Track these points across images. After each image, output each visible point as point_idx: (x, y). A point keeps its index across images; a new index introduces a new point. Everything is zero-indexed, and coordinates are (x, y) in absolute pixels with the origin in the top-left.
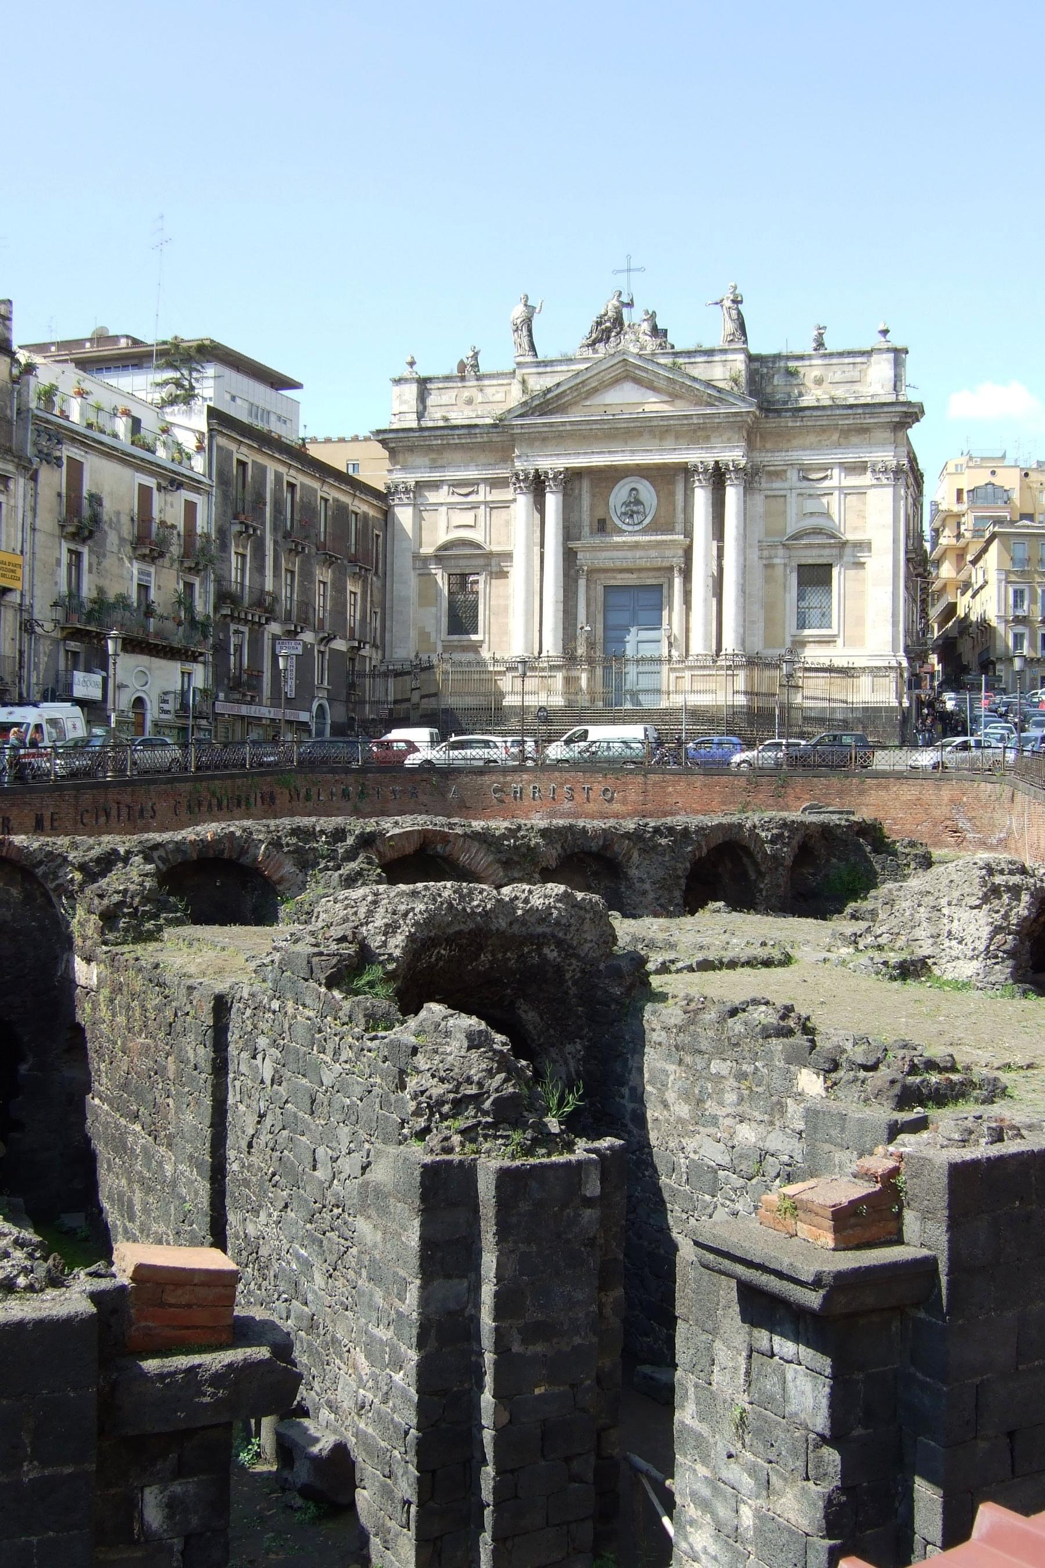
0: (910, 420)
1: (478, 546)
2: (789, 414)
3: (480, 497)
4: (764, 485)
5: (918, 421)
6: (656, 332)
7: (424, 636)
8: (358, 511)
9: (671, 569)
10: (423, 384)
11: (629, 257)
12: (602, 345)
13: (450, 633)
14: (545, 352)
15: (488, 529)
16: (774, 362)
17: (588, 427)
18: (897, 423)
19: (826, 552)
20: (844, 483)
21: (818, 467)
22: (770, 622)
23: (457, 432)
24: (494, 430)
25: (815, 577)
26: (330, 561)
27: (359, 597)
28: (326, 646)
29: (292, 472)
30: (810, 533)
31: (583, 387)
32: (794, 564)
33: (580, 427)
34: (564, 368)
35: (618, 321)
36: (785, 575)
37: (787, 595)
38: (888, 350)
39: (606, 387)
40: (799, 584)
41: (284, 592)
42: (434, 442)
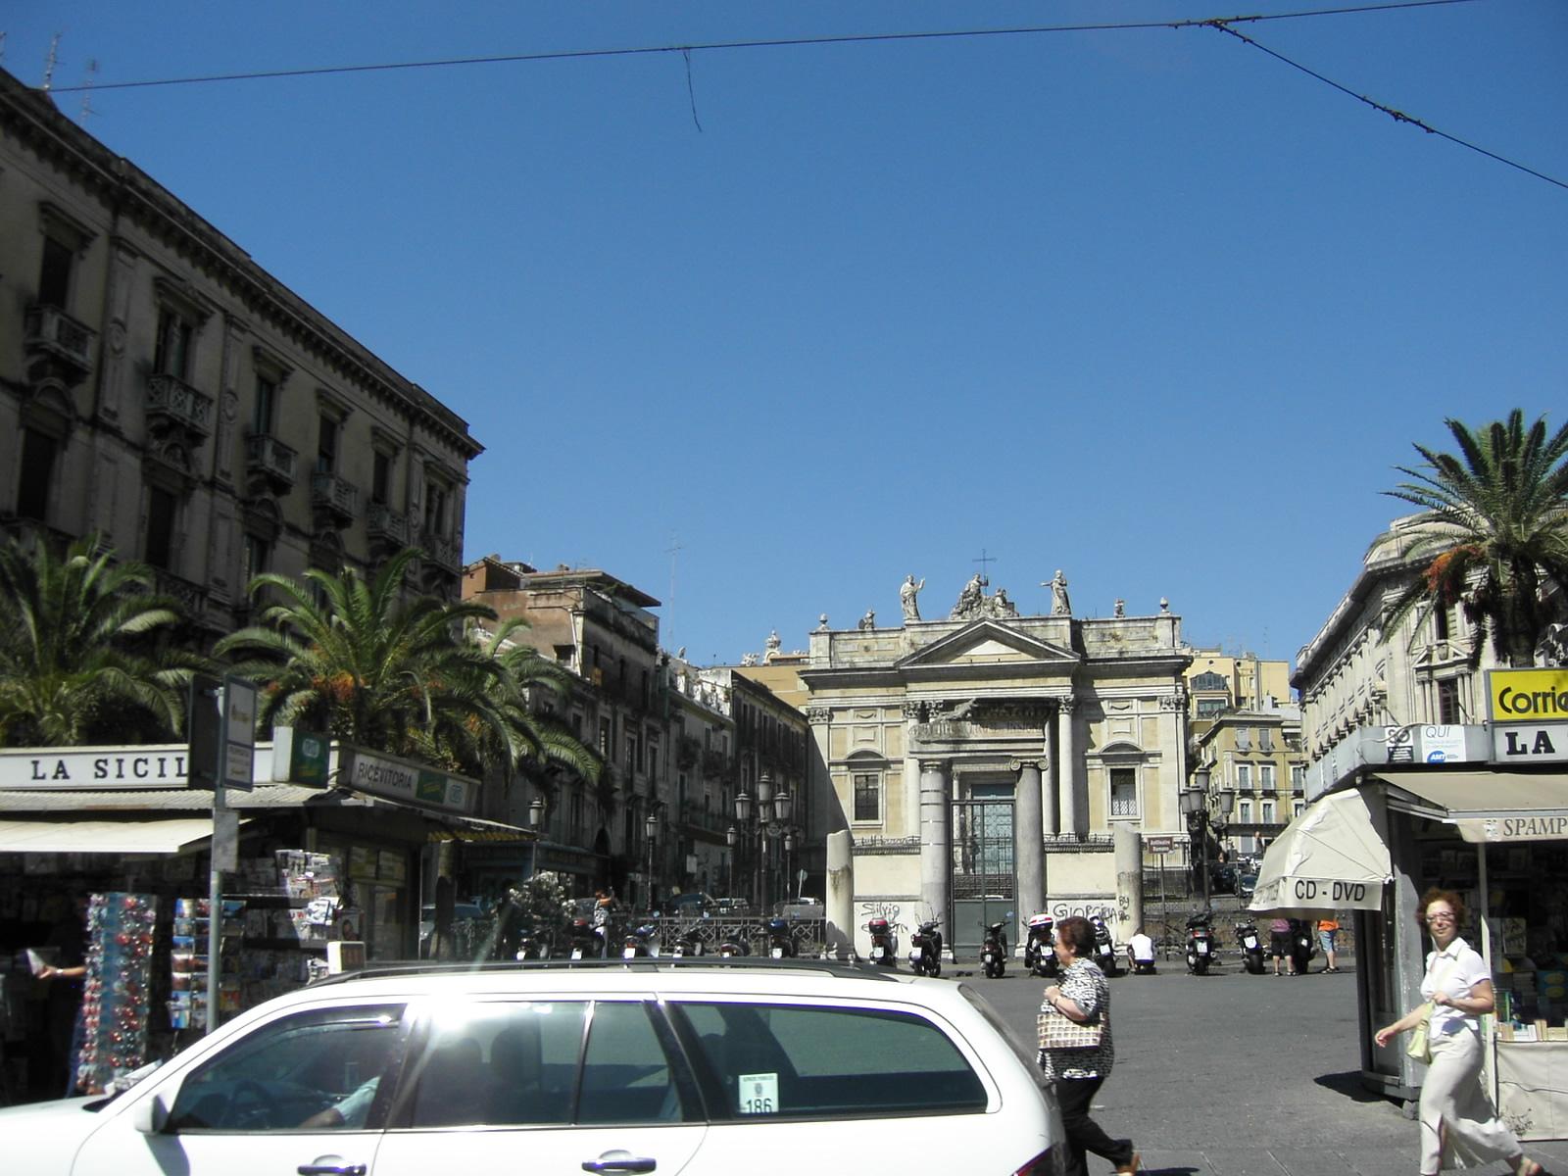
13: (856, 819)
34: (940, 628)
35: (978, 595)
38: (1168, 618)
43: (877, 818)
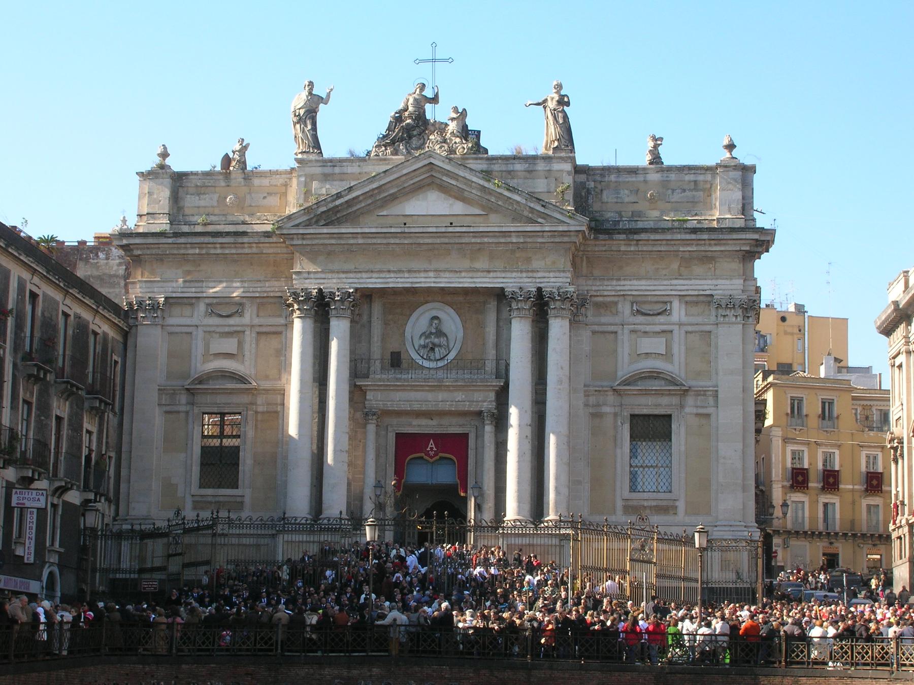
0: (760, 249)
1: (242, 379)
2: (623, 236)
4: (591, 319)
5: (767, 251)
7: (169, 488)
8: (99, 331)
9: (480, 414)
10: (179, 179)
11: (434, 45)
13: (201, 486)
14: (330, 150)
16: (602, 176)
17: (385, 241)
18: (747, 252)
19: (665, 400)
20: (684, 319)
21: (655, 299)
22: (596, 482)
23: (220, 240)
24: (267, 240)
25: (652, 429)
26: (69, 393)
27: (94, 437)
28: (59, 497)
29: (36, 280)
30: (645, 378)
31: (379, 193)
32: (627, 414)
33: (374, 241)
36: (615, 427)
37: (619, 451)
39: (407, 194)
40: (632, 438)
41: (20, 428)
42: (191, 251)
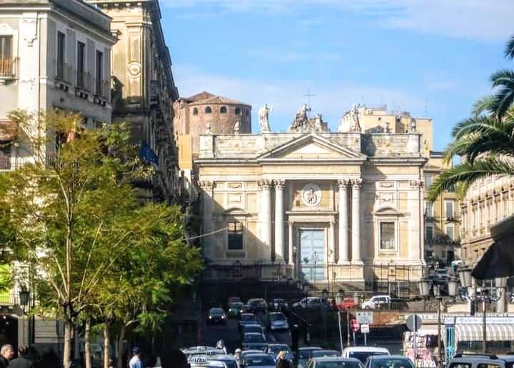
3: (243, 189)
6: (324, 125)
12: (300, 128)
15: (246, 201)
19: (392, 218)
25: (388, 230)
35: (305, 117)
38: (416, 135)
43: (241, 247)
